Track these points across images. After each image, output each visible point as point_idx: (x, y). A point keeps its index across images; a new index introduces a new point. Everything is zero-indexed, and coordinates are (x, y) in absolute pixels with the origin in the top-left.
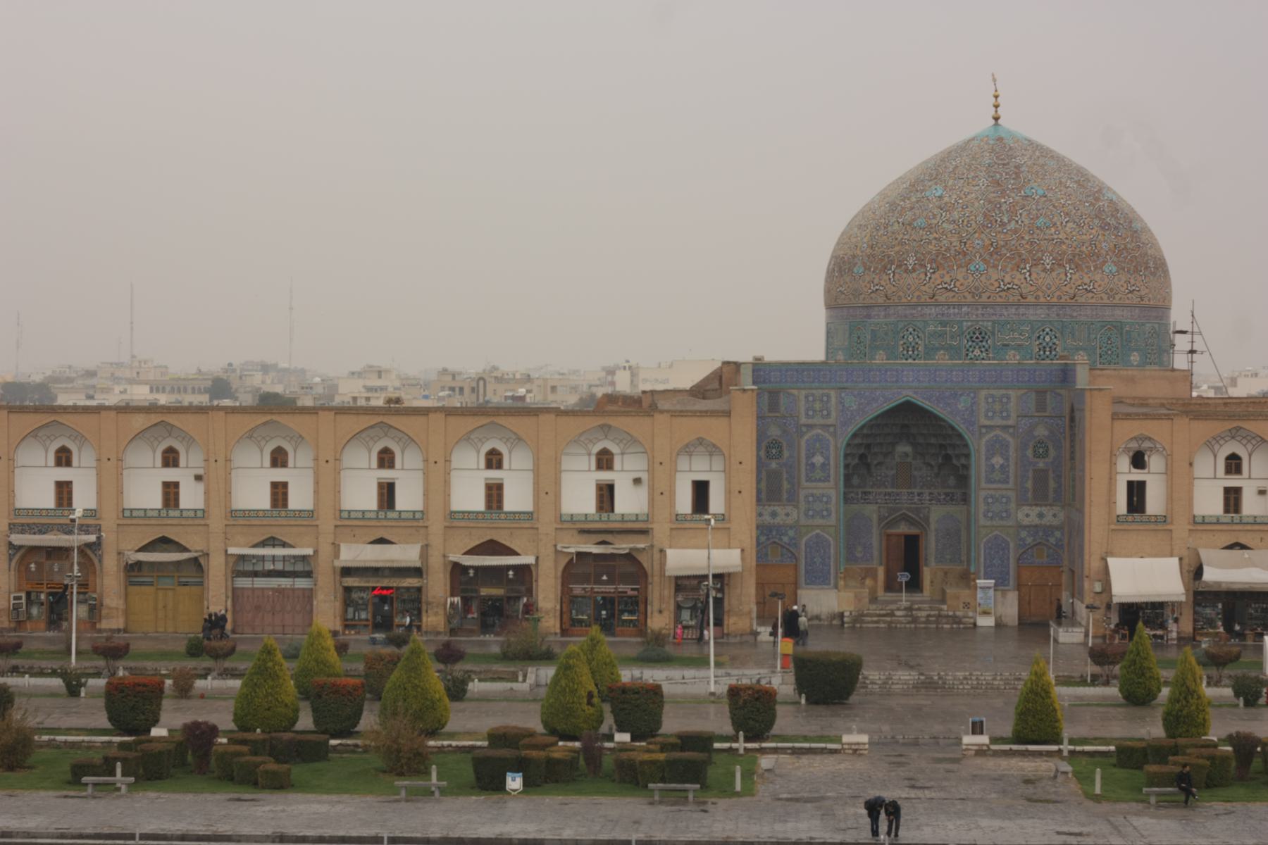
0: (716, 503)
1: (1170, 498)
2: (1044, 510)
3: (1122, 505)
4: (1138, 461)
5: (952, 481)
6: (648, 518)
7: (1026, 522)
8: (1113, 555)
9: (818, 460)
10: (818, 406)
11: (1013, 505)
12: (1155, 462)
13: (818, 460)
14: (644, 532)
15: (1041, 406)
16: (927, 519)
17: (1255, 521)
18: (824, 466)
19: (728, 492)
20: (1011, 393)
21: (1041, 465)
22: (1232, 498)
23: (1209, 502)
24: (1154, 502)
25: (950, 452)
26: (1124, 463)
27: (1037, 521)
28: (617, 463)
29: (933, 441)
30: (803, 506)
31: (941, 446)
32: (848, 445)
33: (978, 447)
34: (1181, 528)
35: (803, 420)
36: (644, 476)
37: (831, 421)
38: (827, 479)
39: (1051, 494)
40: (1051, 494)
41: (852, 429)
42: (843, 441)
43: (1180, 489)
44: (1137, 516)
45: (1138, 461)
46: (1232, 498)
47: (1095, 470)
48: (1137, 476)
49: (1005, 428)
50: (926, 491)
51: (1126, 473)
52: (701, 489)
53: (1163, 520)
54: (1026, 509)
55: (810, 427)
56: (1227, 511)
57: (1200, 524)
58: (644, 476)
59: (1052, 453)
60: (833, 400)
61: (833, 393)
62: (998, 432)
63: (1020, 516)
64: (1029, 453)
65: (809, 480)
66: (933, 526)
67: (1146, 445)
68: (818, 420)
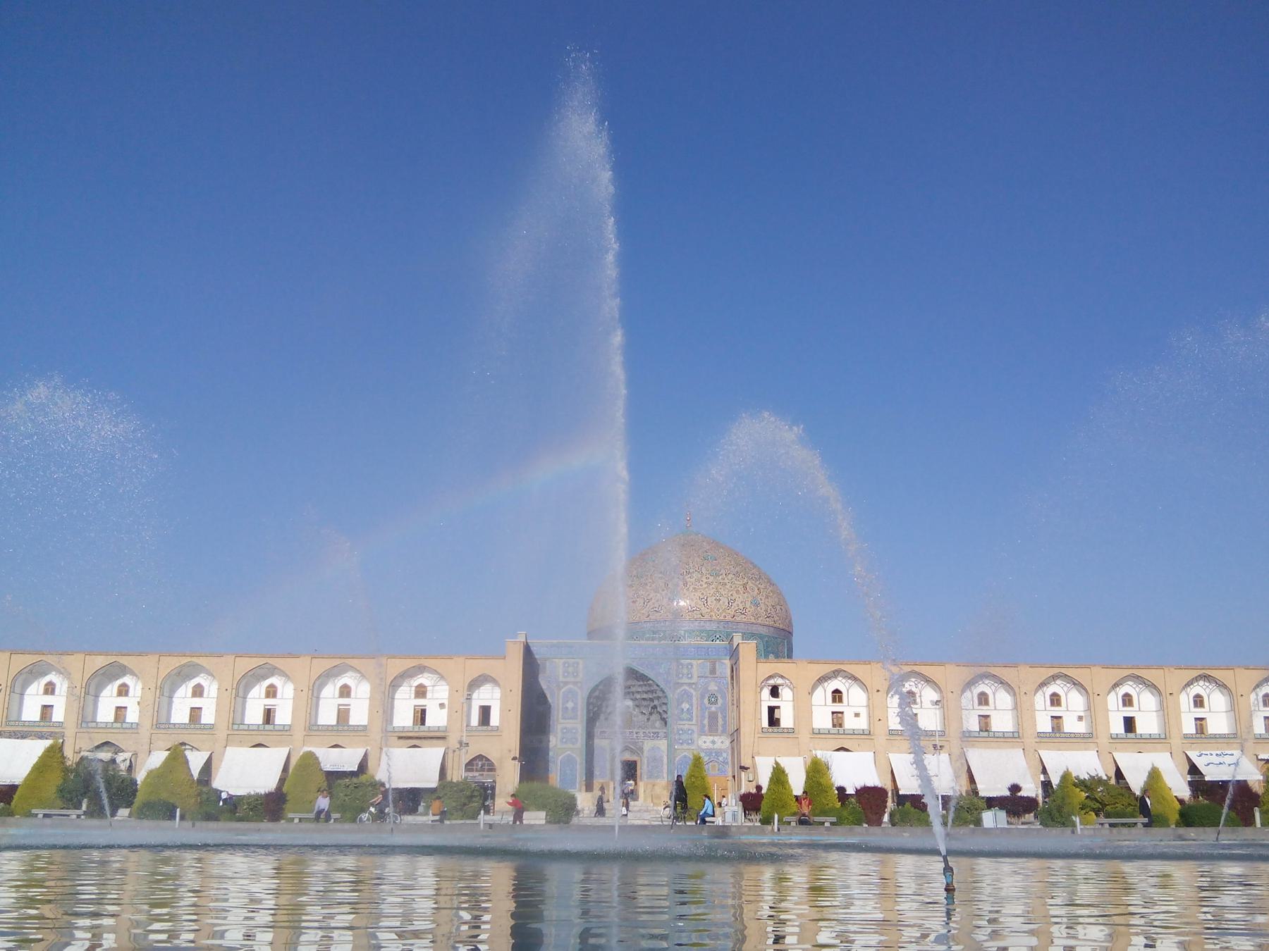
0: (495, 720)
1: (796, 718)
2: (716, 739)
3: (765, 723)
4: (775, 692)
5: (658, 724)
6: (446, 729)
7: (704, 746)
8: (759, 754)
9: (570, 705)
10: (571, 669)
11: (695, 735)
12: (785, 693)
13: (570, 705)
14: (443, 738)
15: (713, 671)
16: (641, 749)
17: (854, 733)
18: (574, 709)
19: (502, 711)
20: (694, 662)
21: (713, 709)
22: (837, 718)
23: (822, 720)
24: (786, 718)
25: (656, 702)
26: (766, 692)
27: (711, 746)
28: (429, 695)
29: (645, 696)
30: (559, 735)
31: (651, 700)
32: (589, 698)
33: (672, 696)
34: (804, 736)
35: (561, 679)
36: (446, 702)
37: (578, 679)
38: (574, 718)
39: (720, 728)
40: (720, 728)
41: (592, 685)
42: (586, 694)
43: (804, 711)
44: (775, 729)
45: (775, 692)
46: (837, 718)
47: (747, 695)
48: (774, 702)
49: (690, 685)
50: (641, 731)
51: (767, 700)
52: (485, 712)
53: (791, 731)
54: (704, 738)
55: (566, 683)
56: (834, 726)
57: (817, 733)
58: (446, 702)
59: (720, 701)
60: (581, 666)
61: (581, 662)
62: (686, 687)
63: (700, 742)
64: (706, 701)
65: (564, 718)
66: (646, 753)
67: (779, 681)
68: (571, 679)
